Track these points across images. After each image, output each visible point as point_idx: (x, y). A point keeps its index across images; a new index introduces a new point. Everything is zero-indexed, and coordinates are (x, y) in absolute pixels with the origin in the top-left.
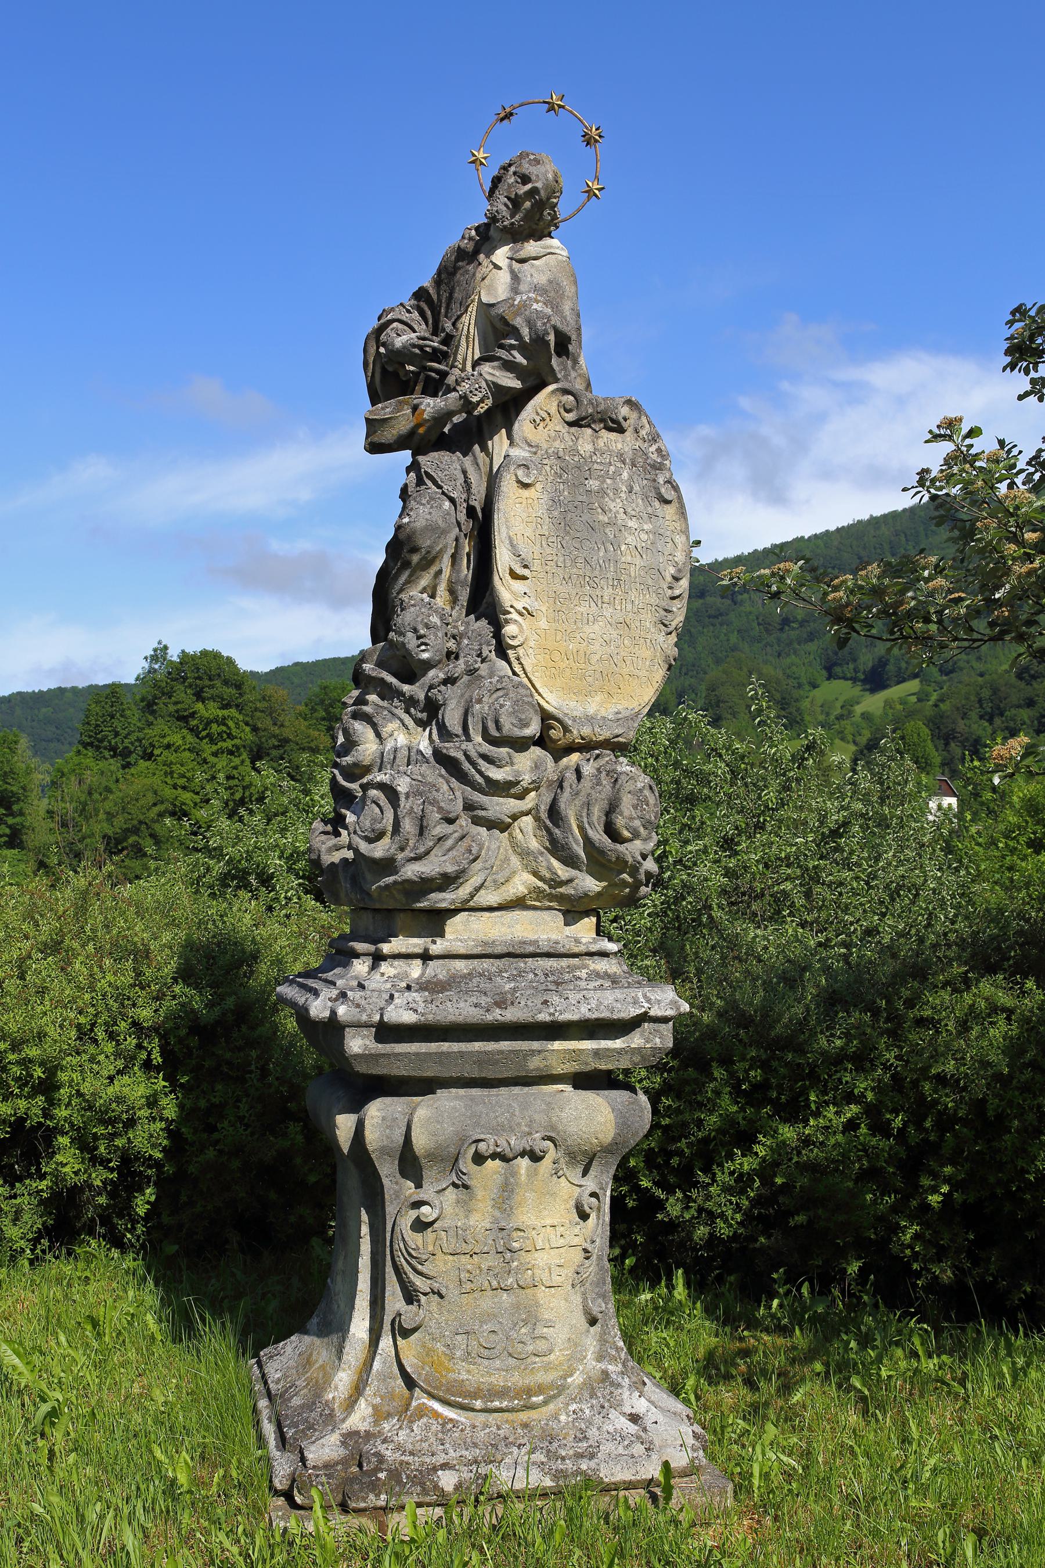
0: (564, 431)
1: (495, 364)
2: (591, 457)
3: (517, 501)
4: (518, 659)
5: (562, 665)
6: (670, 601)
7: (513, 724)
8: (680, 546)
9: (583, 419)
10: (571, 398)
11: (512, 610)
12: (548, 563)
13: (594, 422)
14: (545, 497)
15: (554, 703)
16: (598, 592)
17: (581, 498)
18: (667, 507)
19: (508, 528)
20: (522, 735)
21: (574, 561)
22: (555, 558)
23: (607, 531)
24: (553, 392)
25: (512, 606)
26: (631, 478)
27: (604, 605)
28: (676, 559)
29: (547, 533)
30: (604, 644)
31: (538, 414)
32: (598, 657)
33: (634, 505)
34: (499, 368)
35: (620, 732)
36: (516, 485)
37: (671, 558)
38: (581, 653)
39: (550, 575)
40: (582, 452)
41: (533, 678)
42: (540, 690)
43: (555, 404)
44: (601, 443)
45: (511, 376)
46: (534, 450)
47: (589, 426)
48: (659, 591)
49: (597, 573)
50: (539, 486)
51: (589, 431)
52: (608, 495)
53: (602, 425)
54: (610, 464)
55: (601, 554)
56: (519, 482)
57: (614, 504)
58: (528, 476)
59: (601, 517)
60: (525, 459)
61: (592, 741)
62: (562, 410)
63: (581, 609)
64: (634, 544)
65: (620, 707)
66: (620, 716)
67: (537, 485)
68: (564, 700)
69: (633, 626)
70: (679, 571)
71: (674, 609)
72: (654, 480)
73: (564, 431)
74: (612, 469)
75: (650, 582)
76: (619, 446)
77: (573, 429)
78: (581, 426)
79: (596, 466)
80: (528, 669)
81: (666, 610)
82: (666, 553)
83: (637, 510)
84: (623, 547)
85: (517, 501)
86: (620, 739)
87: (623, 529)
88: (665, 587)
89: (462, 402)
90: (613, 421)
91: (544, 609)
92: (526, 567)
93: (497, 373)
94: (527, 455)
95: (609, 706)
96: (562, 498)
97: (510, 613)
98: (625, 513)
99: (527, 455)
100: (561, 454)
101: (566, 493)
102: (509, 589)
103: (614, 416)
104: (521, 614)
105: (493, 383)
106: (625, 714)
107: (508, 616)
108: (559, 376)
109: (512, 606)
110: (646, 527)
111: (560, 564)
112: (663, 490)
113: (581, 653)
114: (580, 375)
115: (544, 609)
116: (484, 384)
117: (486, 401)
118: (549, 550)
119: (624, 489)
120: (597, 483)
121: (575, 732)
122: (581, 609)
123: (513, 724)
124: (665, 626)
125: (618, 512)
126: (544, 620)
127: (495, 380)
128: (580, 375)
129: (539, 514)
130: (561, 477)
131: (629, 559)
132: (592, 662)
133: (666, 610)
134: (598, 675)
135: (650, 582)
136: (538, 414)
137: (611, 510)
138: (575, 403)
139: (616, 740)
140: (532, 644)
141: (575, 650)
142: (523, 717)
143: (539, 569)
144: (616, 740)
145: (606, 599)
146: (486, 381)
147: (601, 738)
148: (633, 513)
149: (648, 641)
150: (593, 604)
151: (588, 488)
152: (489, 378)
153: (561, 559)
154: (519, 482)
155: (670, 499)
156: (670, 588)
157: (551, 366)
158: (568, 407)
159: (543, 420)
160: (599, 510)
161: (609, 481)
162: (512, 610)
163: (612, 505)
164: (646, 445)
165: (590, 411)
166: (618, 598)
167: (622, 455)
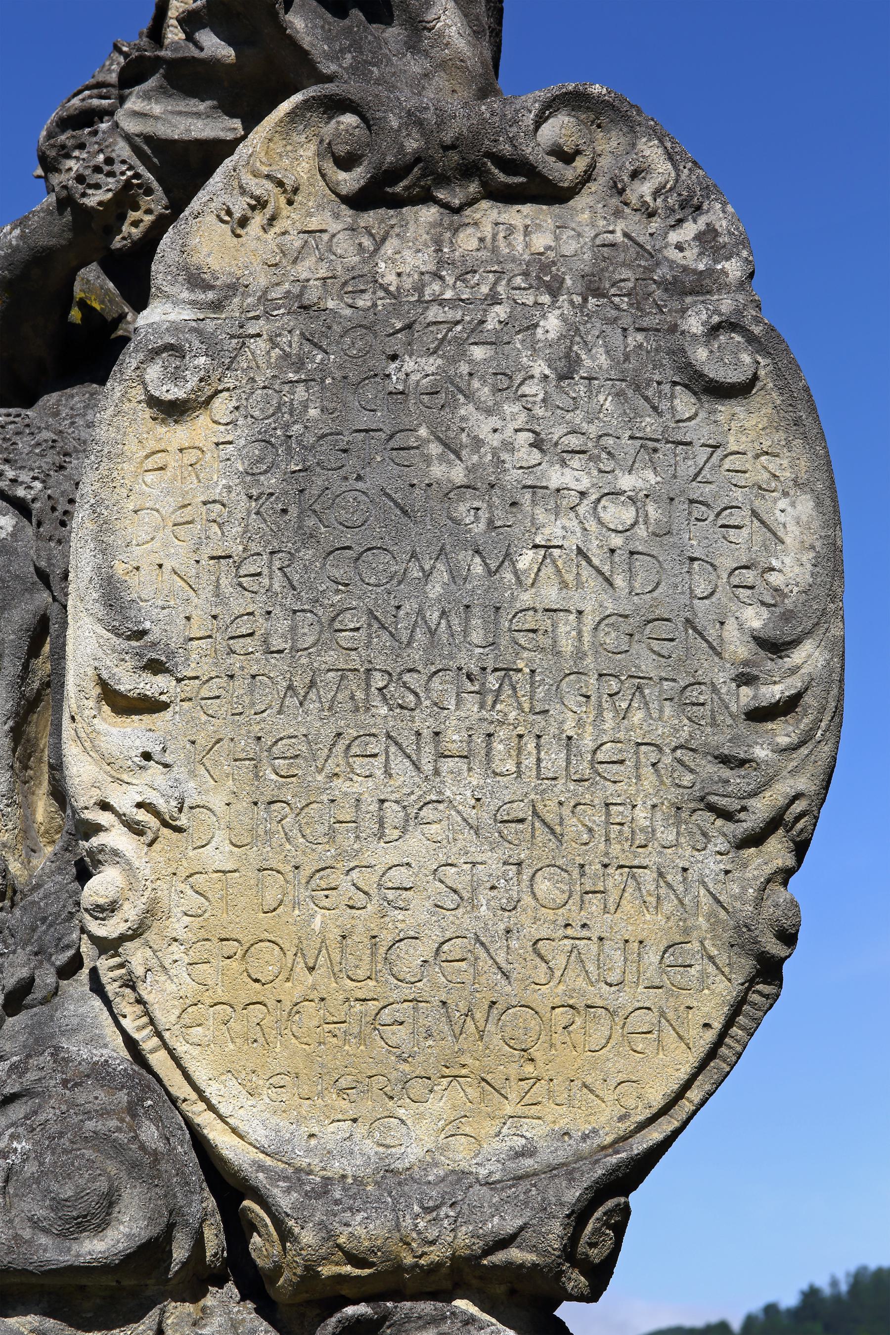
0: (334, 226)
1: (152, 83)
2: (419, 288)
3: (150, 464)
4: (130, 983)
5: (291, 992)
6: (743, 728)
7: (35, 1223)
8: (792, 536)
9: (393, 175)
10: (349, 119)
11: (104, 818)
12: (237, 645)
13: (443, 180)
14: (241, 434)
15: (259, 1134)
16: (424, 722)
17: (364, 420)
18: (724, 409)
19: (104, 549)
20: (65, 1259)
21: (332, 625)
22: (261, 625)
23: (462, 510)
24: (293, 115)
25: (105, 806)
26: (572, 332)
27: (446, 765)
28: (774, 579)
29: (237, 549)
30: (450, 901)
31: (243, 191)
32: (425, 949)
33: (577, 418)
34: (162, 92)
35: (511, 1224)
36: (148, 413)
37: (749, 577)
38: (360, 936)
39: (240, 686)
40: (390, 279)
41: (181, 1048)
42: (212, 1091)
43: (309, 151)
44: (467, 241)
45: (202, 107)
46: (211, 295)
47: (426, 198)
48: (693, 694)
49: (415, 655)
50: (222, 406)
51: (428, 213)
52: (469, 396)
53: (473, 188)
54: (494, 299)
55: (435, 590)
56: (153, 402)
57: (494, 421)
58: (176, 377)
59: (437, 471)
60: (175, 328)
61: (399, 1268)
62: (329, 166)
63: (359, 786)
64: (571, 543)
65: (535, 1130)
66: (528, 1163)
67: (217, 402)
68: (299, 1121)
69: (573, 826)
70: (788, 616)
71: (761, 753)
72: (673, 329)
73: (334, 226)
74: (500, 311)
75: (648, 665)
76: (540, 241)
77: (370, 218)
78: (397, 203)
79: (434, 313)
80: (163, 1019)
81: (725, 760)
82: (726, 563)
83: (593, 430)
84: (526, 560)
85: (150, 464)
86: (515, 1254)
87: (526, 497)
88: (722, 677)
89: (68, 216)
90: (510, 165)
91: (217, 801)
92: (155, 667)
93: (157, 109)
94: (187, 314)
95: (489, 1127)
96: (297, 429)
97: (97, 829)
98: (538, 444)
99: (187, 314)
100: (312, 295)
101: (313, 412)
102: (92, 748)
103: (506, 149)
104: (135, 828)
105: (149, 139)
106: (547, 1155)
107: (95, 841)
108: (328, 68)
109: (105, 806)
110: (626, 482)
111: (277, 643)
112: (700, 354)
113: (360, 936)
114: (443, 65)
115: (217, 801)
116: (122, 150)
117: (145, 201)
118: (239, 604)
119: (540, 368)
120: (432, 364)
121: (308, 1237)
122: (359, 786)
123: (35, 1223)
124: (726, 815)
125: (508, 446)
126: (221, 838)
127: (147, 128)
128: (443, 65)
129: (216, 493)
130: (299, 365)
131: (550, 594)
132: (403, 970)
133: (725, 760)
134: (430, 1017)
135: (648, 665)
136: (243, 191)
137: (477, 443)
138: (361, 133)
139: (499, 1257)
140: (177, 926)
141: (334, 934)
142: (68, 1191)
143: (205, 669)
144: (499, 1257)
145: (454, 739)
146: (128, 138)
147: (435, 1254)
148: (574, 442)
149: (648, 877)
150: (399, 764)
151: (396, 383)
152: (132, 126)
153: (283, 625)
154: (153, 402)
155: (733, 376)
156: (745, 679)
157: (293, 44)
158: (341, 150)
159: (260, 204)
160: (435, 449)
161: (478, 353)
162: (104, 818)
163: (483, 426)
164: (655, 225)
165: (412, 145)
166: (502, 733)
167: (545, 268)
